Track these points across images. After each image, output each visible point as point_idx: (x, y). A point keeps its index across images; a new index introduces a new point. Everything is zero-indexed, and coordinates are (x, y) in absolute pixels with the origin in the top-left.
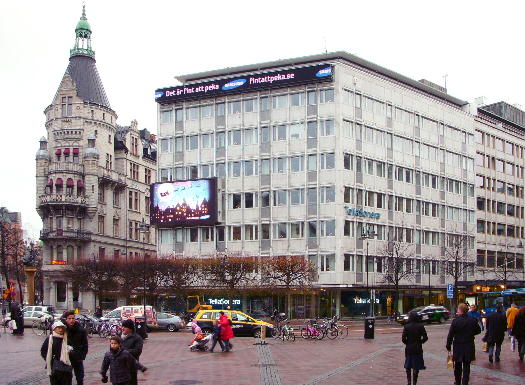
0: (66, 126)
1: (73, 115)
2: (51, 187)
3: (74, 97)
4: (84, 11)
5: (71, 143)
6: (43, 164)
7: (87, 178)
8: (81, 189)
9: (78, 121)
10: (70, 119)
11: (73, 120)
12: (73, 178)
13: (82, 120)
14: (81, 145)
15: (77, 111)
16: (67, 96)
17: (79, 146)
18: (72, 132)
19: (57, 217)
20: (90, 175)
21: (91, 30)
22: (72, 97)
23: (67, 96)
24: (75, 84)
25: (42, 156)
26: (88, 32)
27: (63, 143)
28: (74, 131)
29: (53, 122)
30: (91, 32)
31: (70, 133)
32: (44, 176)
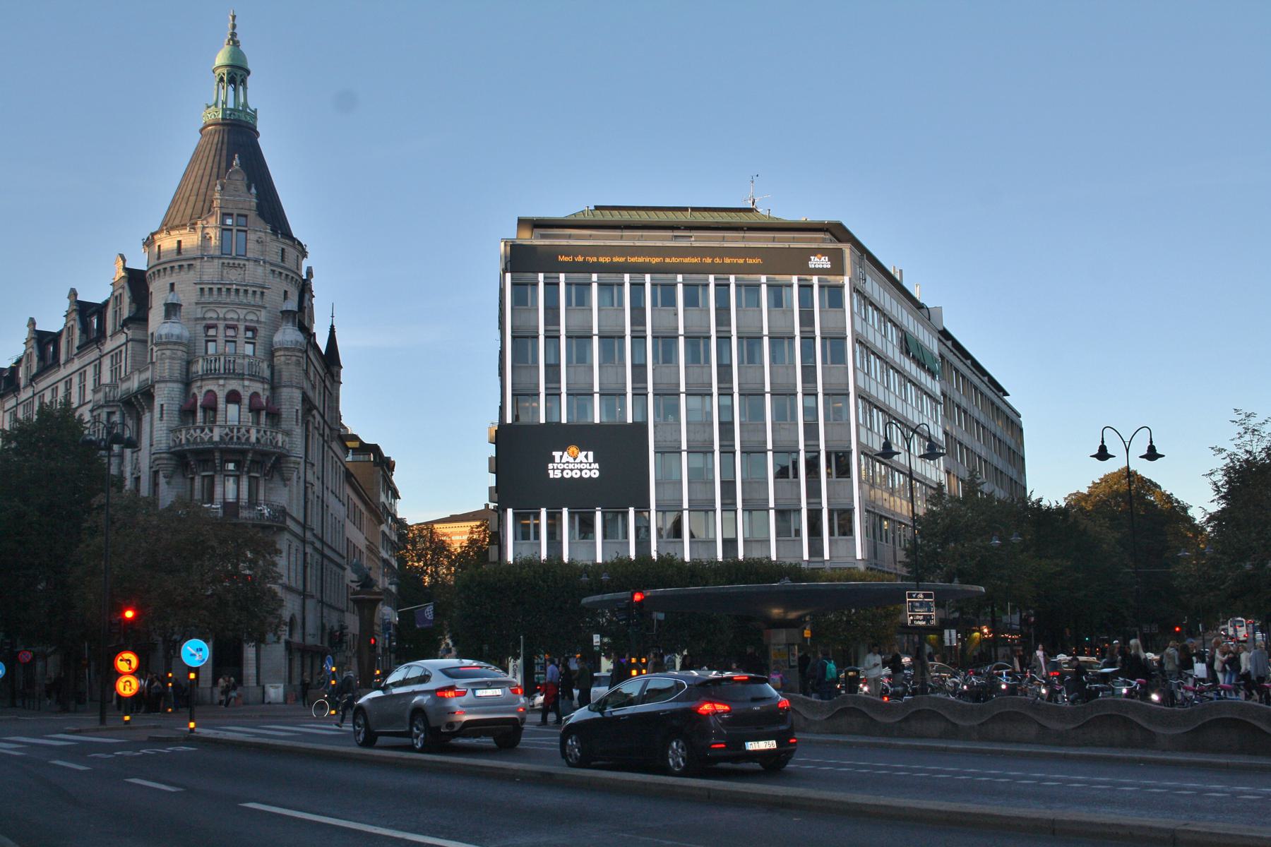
0: (233, 276)
1: (250, 255)
2: (211, 407)
3: (252, 215)
4: (234, 27)
5: (242, 313)
6: (180, 353)
7: (285, 393)
8: (274, 416)
9: (260, 270)
10: (242, 262)
11: (250, 265)
12: (261, 393)
13: (269, 268)
14: (263, 319)
15: (257, 247)
16: (235, 212)
17: (258, 321)
18: (246, 291)
19: (204, 477)
20: (292, 386)
21: (250, 67)
22: (246, 216)
23: (235, 212)
24: (253, 190)
25: (178, 337)
26: (240, 72)
27: (221, 312)
28: (251, 290)
29: (197, 263)
30: (248, 72)
31: (258, 295)
32: (181, 382)
